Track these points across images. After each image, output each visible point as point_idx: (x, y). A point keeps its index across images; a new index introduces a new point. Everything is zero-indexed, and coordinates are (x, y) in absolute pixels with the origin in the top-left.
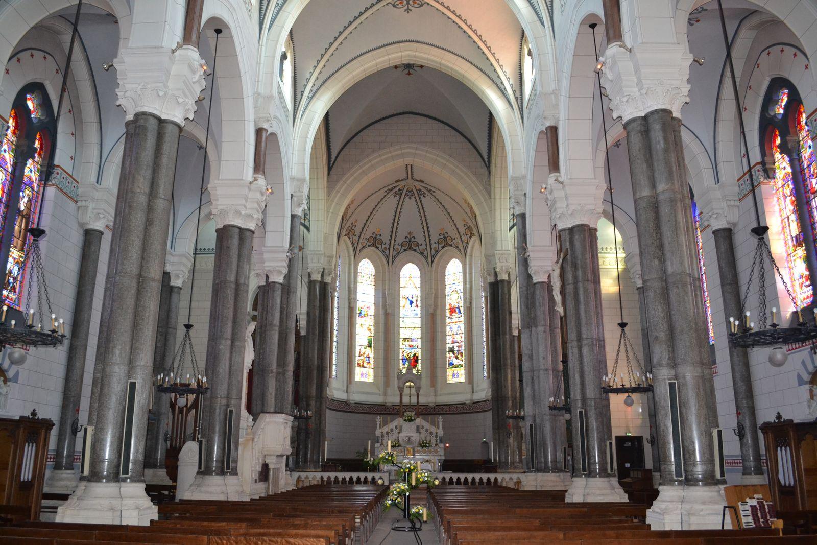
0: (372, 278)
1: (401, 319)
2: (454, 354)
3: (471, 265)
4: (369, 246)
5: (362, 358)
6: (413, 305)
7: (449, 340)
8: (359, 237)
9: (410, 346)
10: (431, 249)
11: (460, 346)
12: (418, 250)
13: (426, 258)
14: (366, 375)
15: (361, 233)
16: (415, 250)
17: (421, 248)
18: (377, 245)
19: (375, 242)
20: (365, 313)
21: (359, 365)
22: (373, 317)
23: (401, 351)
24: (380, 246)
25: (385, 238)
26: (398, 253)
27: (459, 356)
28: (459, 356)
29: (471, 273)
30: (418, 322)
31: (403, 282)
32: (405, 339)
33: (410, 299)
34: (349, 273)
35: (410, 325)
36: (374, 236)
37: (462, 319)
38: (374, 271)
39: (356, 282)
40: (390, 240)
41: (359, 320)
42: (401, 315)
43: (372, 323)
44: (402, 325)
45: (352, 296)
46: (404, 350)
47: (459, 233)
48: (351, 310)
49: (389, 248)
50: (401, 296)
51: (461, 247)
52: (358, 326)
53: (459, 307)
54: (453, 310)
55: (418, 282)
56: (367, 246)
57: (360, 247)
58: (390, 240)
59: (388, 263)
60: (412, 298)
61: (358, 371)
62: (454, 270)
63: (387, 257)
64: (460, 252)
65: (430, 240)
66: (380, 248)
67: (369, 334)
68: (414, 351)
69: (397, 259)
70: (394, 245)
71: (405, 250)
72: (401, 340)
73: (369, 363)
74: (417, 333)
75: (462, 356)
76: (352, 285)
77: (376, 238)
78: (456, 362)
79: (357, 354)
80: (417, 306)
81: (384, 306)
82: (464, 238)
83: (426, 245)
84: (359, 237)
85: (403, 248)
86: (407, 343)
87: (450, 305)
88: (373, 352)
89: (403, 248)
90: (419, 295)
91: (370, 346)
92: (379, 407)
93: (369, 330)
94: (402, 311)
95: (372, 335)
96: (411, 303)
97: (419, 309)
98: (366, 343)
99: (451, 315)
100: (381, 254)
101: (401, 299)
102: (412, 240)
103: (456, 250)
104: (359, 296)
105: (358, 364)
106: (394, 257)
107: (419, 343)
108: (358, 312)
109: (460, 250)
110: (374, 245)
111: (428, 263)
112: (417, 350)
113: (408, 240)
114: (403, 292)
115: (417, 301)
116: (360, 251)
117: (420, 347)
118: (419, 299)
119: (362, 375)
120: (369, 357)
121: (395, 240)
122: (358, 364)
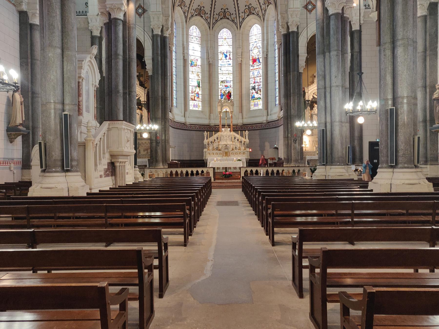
2: (255, 90)
3: (267, 27)
4: (196, 15)
6: (227, 58)
7: (252, 81)
8: (189, 8)
9: (226, 86)
10: (239, 17)
11: (260, 85)
12: (230, 19)
13: (236, 24)
15: (190, 4)
16: (228, 19)
19: (200, 12)
22: (200, 67)
23: (220, 90)
24: (204, 16)
25: (207, 9)
26: (217, 21)
27: (259, 92)
28: (259, 92)
29: (267, 33)
31: (220, 42)
32: (222, 82)
33: (225, 53)
34: (183, 35)
35: (225, 72)
36: (199, 8)
37: (261, 66)
39: (188, 42)
40: (211, 11)
41: (191, 69)
42: (219, 65)
43: (199, 70)
45: (185, 51)
46: (221, 88)
47: (260, 3)
48: (185, 61)
50: (219, 52)
51: (260, 14)
52: (190, 73)
53: (258, 58)
54: (254, 61)
55: (230, 42)
56: (195, 15)
57: (189, 15)
58: (211, 11)
60: (227, 53)
61: (191, 103)
62: (256, 32)
63: (209, 24)
64: (260, 18)
65: (239, 10)
66: (204, 17)
68: (228, 90)
71: (221, 19)
73: (198, 97)
74: (230, 78)
75: (260, 91)
76: (185, 44)
78: (256, 96)
79: (190, 92)
80: (230, 58)
82: (263, 7)
84: (189, 8)
87: (253, 56)
90: (231, 51)
91: (199, 86)
93: (198, 75)
94: (220, 62)
95: (200, 79)
96: (226, 56)
99: (253, 64)
100: (204, 22)
101: (219, 54)
103: (257, 17)
104: (191, 52)
105: (191, 98)
106: (214, 24)
108: (190, 63)
109: (260, 17)
110: (199, 14)
111: (237, 28)
113: (223, 11)
114: (221, 49)
115: (230, 55)
117: (232, 87)
118: (231, 54)
119: (194, 106)
121: (214, 11)
122: (191, 98)
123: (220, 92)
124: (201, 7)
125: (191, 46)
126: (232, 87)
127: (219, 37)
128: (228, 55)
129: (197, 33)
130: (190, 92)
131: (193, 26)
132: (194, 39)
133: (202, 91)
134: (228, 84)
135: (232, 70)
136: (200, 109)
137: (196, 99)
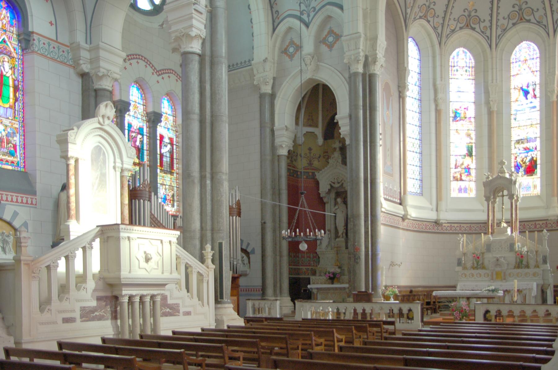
0: (471, 71)
1: (512, 117)
5: (459, 169)
6: (529, 96)
9: (527, 149)
12: (533, 20)
14: (466, 190)
17: (537, 15)
18: (473, 26)
19: (469, 21)
20: (462, 115)
21: (455, 179)
22: (473, 120)
23: (513, 157)
24: (477, 26)
25: (484, 14)
26: (505, 30)
30: (536, 116)
32: (518, 142)
33: (525, 88)
36: (466, 14)
38: (473, 61)
41: (453, 125)
42: (513, 112)
43: (472, 127)
44: (513, 123)
49: (491, 27)
50: (512, 87)
52: (452, 133)
55: (536, 64)
56: (458, 28)
59: (490, 46)
60: (528, 87)
61: (455, 185)
63: (489, 39)
66: (478, 29)
67: (468, 140)
68: (530, 155)
69: (504, 40)
70: (498, 20)
71: (514, 24)
72: (513, 143)
73: (469, 174)
74: (535, 132)
77: (469, 16)
79: (453, 166)
80: (535, 96)
81: (488, 103)
83: (545, 9)
85: (511, 22)
86: (522, 146)
88: (474, 161)
89: (511, 22)
90: (538, 82)
91: (470, 154)
92: (482, 225)
93: (469, 135)
95: (473, 141)
96: (526, 93)
97: (538, 99)
98: (465, 152)
100: (480, 38)
101: (512, 91)
102: (524, 6)
104: (453, 96)
105: (454, 177)
106: (499, 37)
107: (538, 143)
108: (452, 115)
110: (468, 26)
112: (536, 152)
113: (517, 8)
115: (534, 90)
116: (448, 37)
117: (538, 148)
118: (538, 87)
119: (460, 190)
120: (469, 169)
121: (498, 14)
122: (454, 177)
123: (513, 160)
124: (470, 12)
125: (453, 85)
126: (538, 148)
127: (512, 61)
128: (530, 90)
129: (468, 61)
130: (453, 166)
131: (457, 50)
132: (461, 71)
133: (477, 164)
134: (530, 145)
135: (538, 117)
136: (473, 194)
137: (464, 177)
